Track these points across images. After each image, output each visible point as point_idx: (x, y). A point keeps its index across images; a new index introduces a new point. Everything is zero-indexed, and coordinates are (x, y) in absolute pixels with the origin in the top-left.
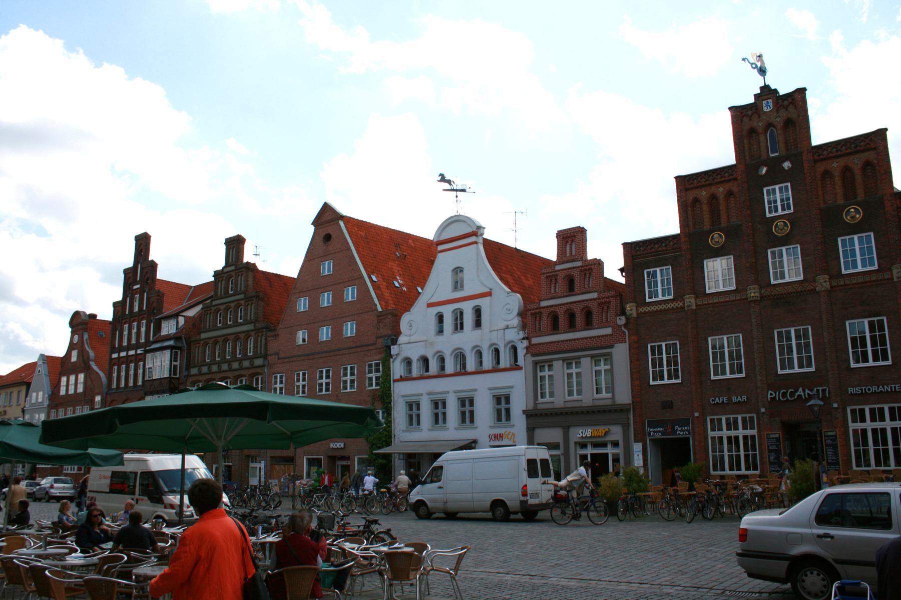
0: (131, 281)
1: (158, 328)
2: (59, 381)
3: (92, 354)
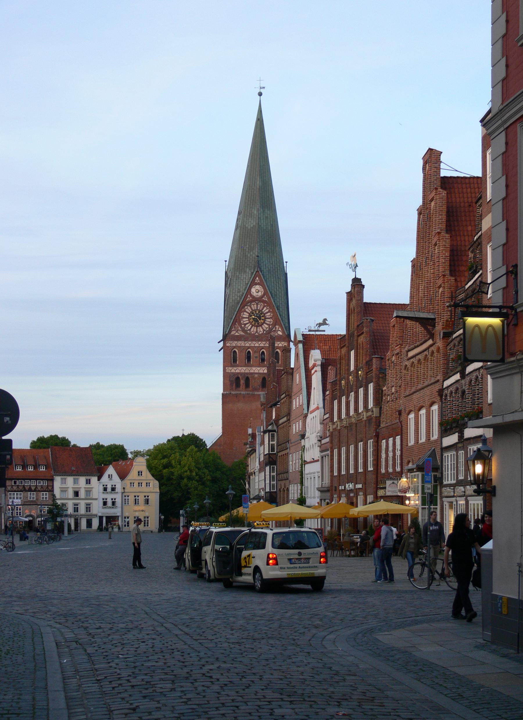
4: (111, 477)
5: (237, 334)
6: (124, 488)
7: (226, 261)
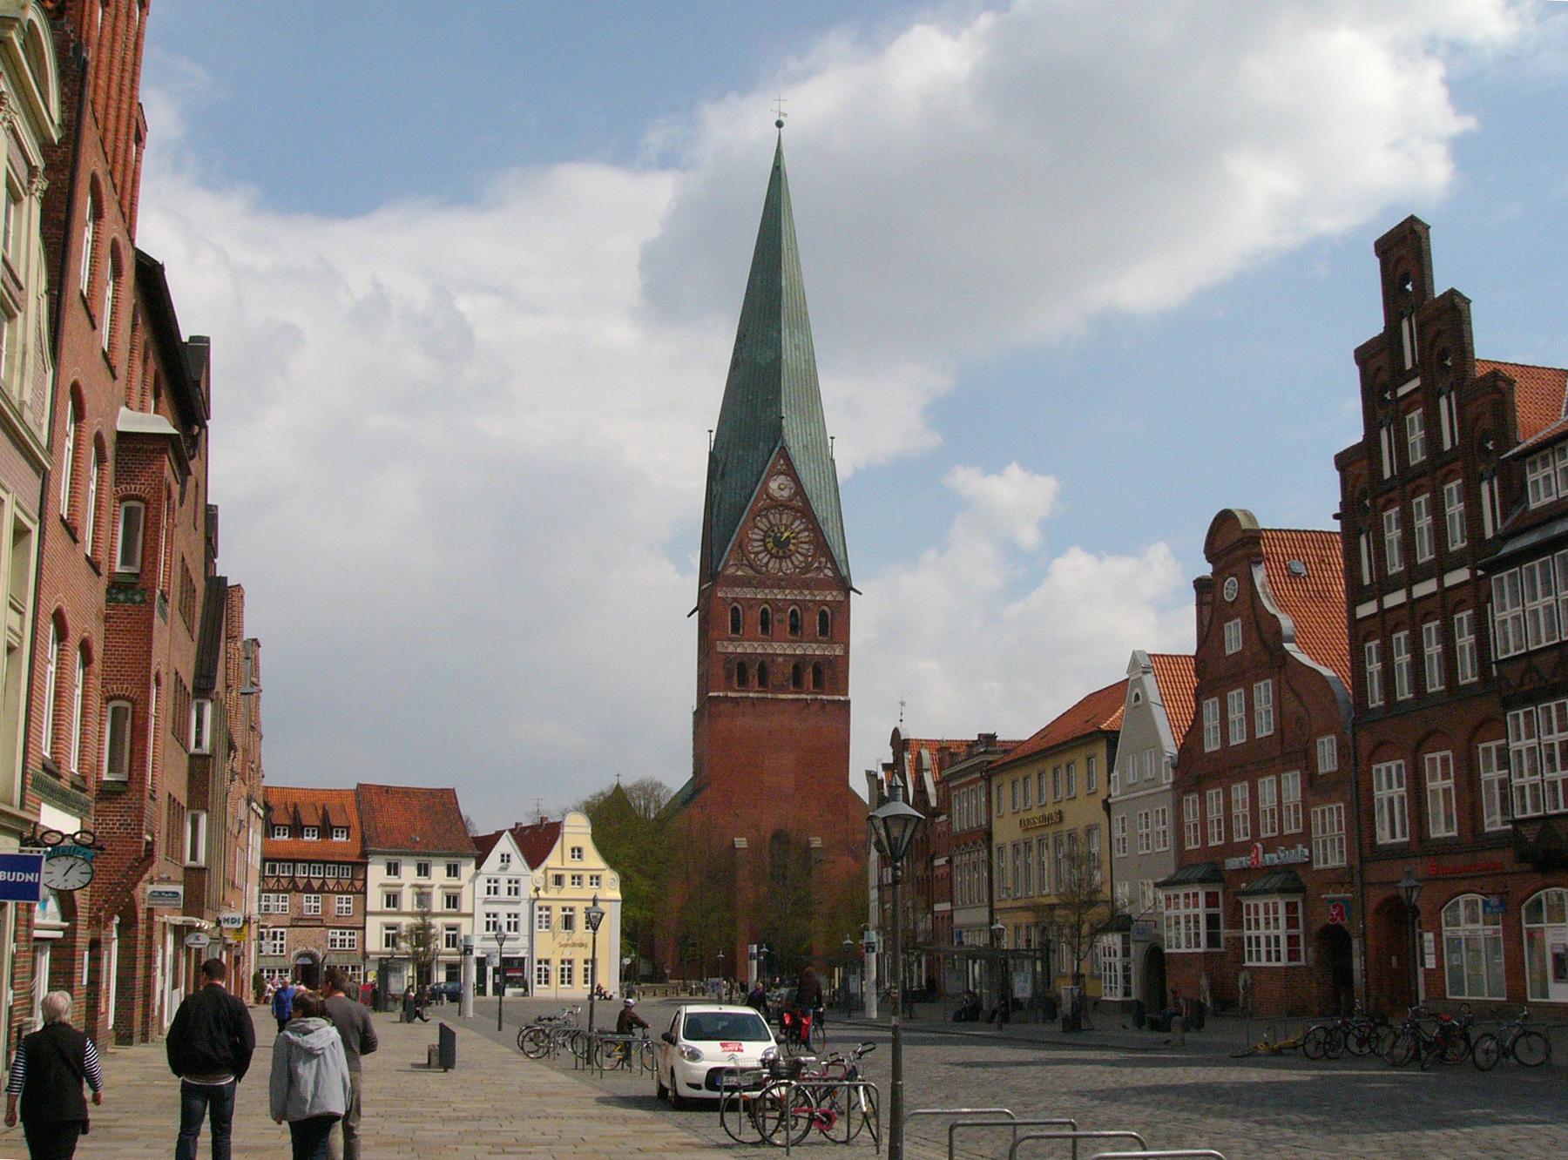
0: (1384, 376)
1: (1514, 493)
2: (1198, 714)
3: (1286, 623)
4: (508, 861)
5: (739, 573)
6: (537, 890)
7: (711, 431)
